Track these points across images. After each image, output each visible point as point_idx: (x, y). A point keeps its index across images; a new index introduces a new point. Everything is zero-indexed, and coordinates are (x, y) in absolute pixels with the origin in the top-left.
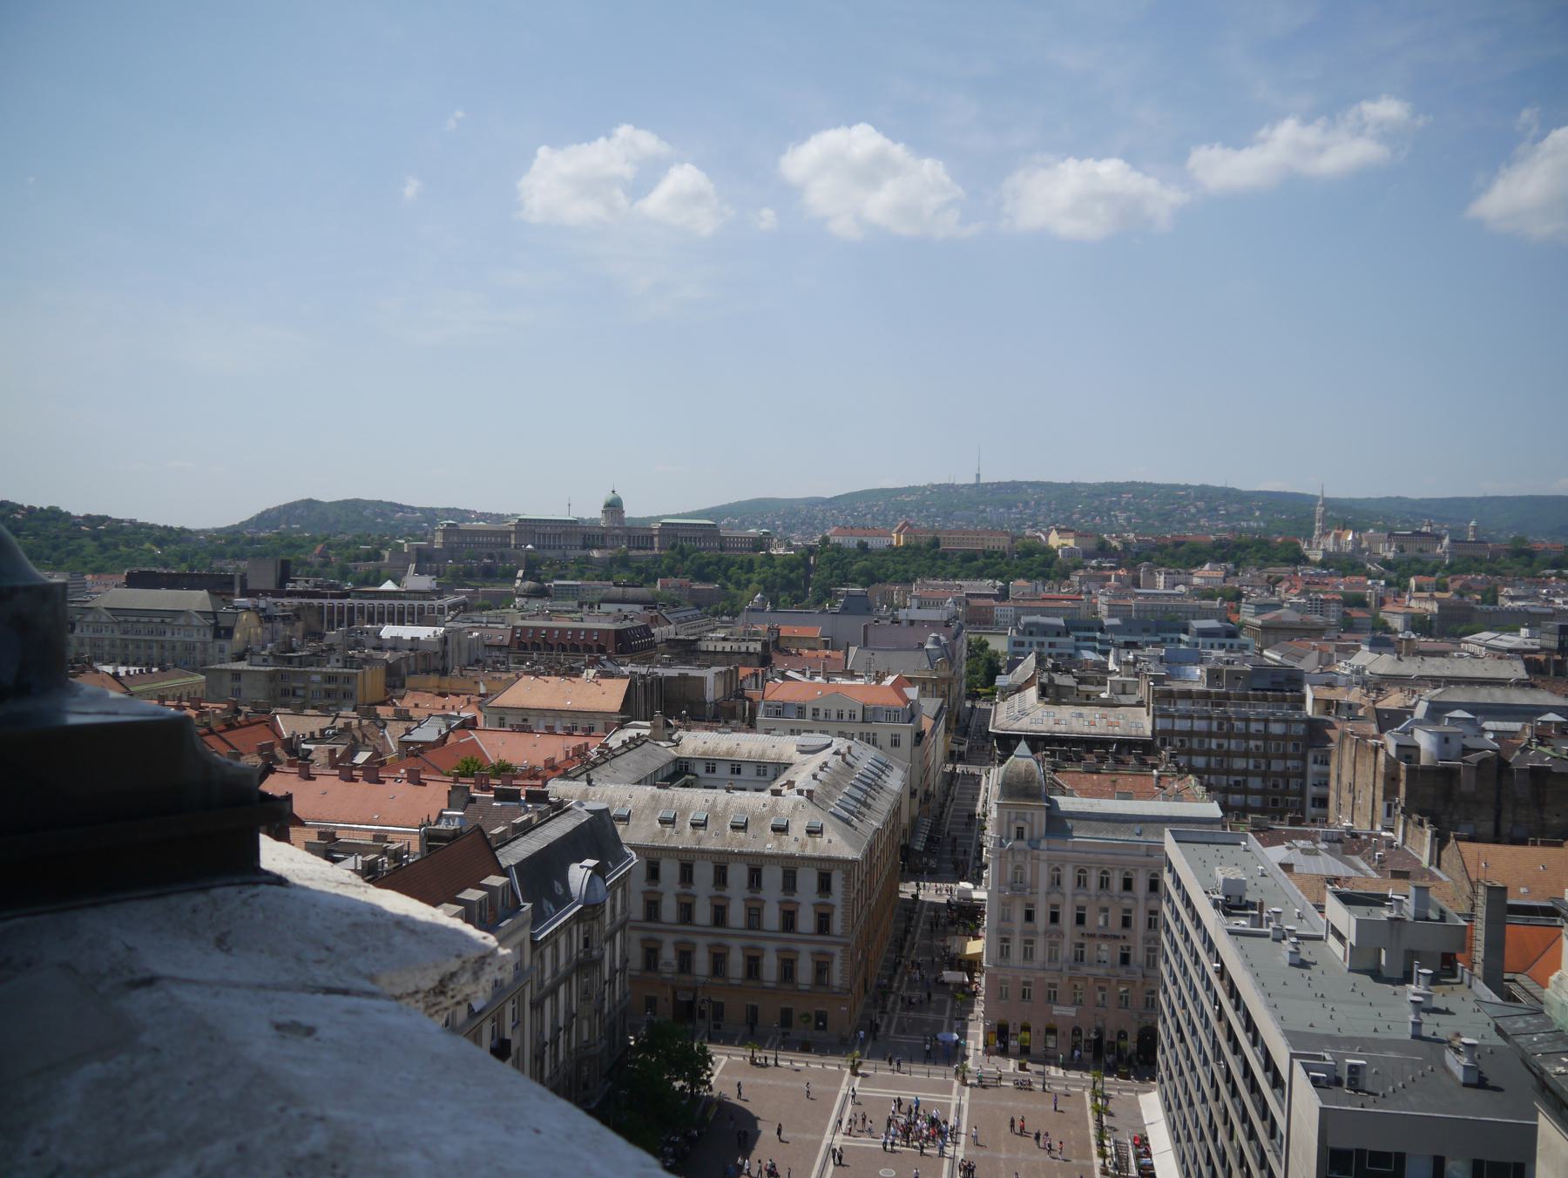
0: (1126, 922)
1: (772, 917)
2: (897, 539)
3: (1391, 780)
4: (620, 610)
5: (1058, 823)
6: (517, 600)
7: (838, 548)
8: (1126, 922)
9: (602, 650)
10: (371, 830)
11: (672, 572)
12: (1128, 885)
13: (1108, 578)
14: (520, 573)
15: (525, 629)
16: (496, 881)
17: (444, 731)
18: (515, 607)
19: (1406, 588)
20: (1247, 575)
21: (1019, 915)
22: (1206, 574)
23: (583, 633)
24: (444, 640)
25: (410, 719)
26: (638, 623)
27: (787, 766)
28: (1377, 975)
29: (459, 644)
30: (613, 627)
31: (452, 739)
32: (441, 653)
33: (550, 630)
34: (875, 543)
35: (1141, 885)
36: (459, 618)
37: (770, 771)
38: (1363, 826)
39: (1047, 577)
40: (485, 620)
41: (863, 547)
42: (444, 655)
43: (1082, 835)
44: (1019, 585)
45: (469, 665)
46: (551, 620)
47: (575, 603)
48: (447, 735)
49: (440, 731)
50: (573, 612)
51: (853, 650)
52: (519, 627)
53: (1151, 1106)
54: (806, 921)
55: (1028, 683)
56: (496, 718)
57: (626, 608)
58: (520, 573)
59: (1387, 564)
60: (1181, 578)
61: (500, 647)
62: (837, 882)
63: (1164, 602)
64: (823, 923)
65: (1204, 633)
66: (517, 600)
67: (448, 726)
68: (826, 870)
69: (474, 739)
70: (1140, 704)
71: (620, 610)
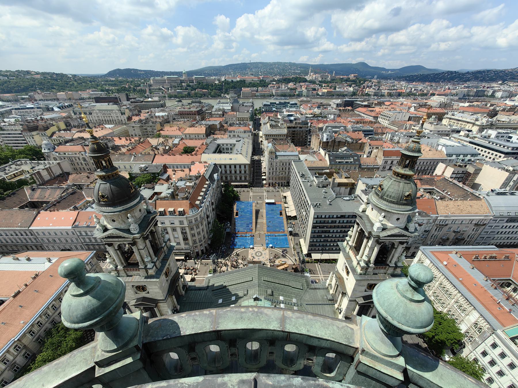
0: (286, 169)
1: (238, 172)
2: (238, 79)
3: (320, 143)
5: (276, 157)
7: (228, 81)
8: (286, 169)
9: (195, 114)
11: (198, 88)
12: (286, 165)
13: (274, 86)
16: (207, 183)
19: (322, 86)
20: (298, 85)
21: (271, 169)
22: (291, 85)
26: (200, 108)
27: (235, 145)
28: (319, 187)
33: (185, 111)
34: (234, 80)
35: (288, 164)
37: (232, 145)
38: (315, 150)
39: (264, 86)
41: (232, 81)
43: (279, 158)
44: (260, 88)
51: (238, 113)
53: (288, 194)
54: (243, 172)
55: (268, 122)
59: (320, 82)
60: (287, 86)
62: (247, 166)
63: (283, 91)
64: (245, 172)
65: (292, 104)
68: (245, 165)
70: (285, 128)
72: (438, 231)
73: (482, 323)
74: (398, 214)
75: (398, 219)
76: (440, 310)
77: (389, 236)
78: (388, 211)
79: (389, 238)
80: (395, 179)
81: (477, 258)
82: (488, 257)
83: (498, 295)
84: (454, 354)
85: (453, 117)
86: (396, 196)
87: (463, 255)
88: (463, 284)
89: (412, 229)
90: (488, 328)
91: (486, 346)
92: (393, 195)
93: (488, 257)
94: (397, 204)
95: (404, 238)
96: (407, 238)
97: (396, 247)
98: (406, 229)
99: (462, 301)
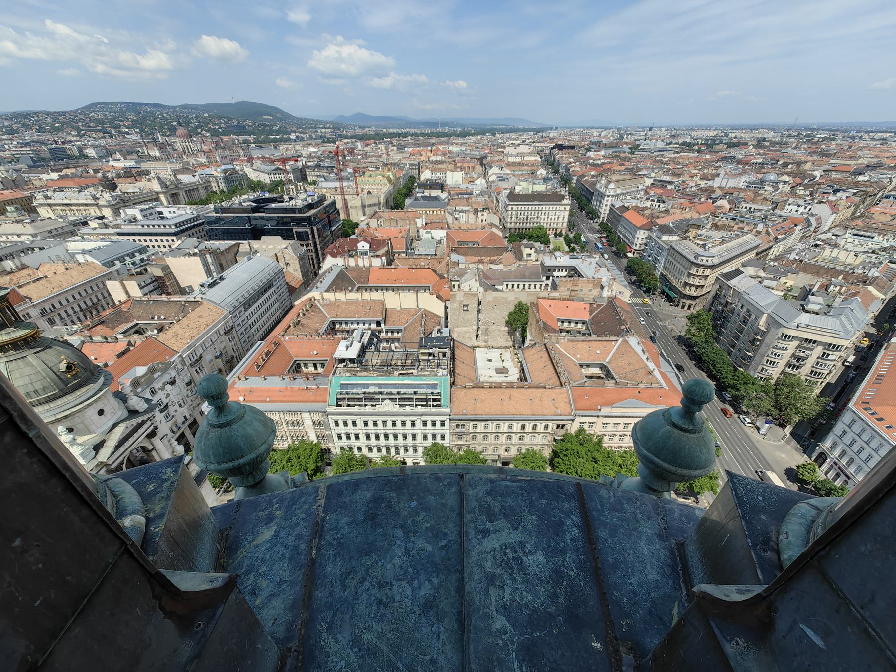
72: (201, 371)
73: (318, 417)
74: (89, 405)
75: (101, 412)
76: (287, 445)
77: (117, 448)
78: (66, 417)
79: (122, 449)
80: (6, 360)
81: (258, 366)
82: (265, 358)
83: (301, 382)
84: (329, 465)
85: (49, 201)
86: (46, 384)
87: (246, 375)
88: (273, 401)
89: (141, 405)
90: (322, 416)
91: (335, 431)
92: (38, 386)
93: (265, 358)
94: (66, 394)
95: (145, 427)
96: (149, 423)
97: (150, 447)
98: (133, 413)
99: (289, 417)
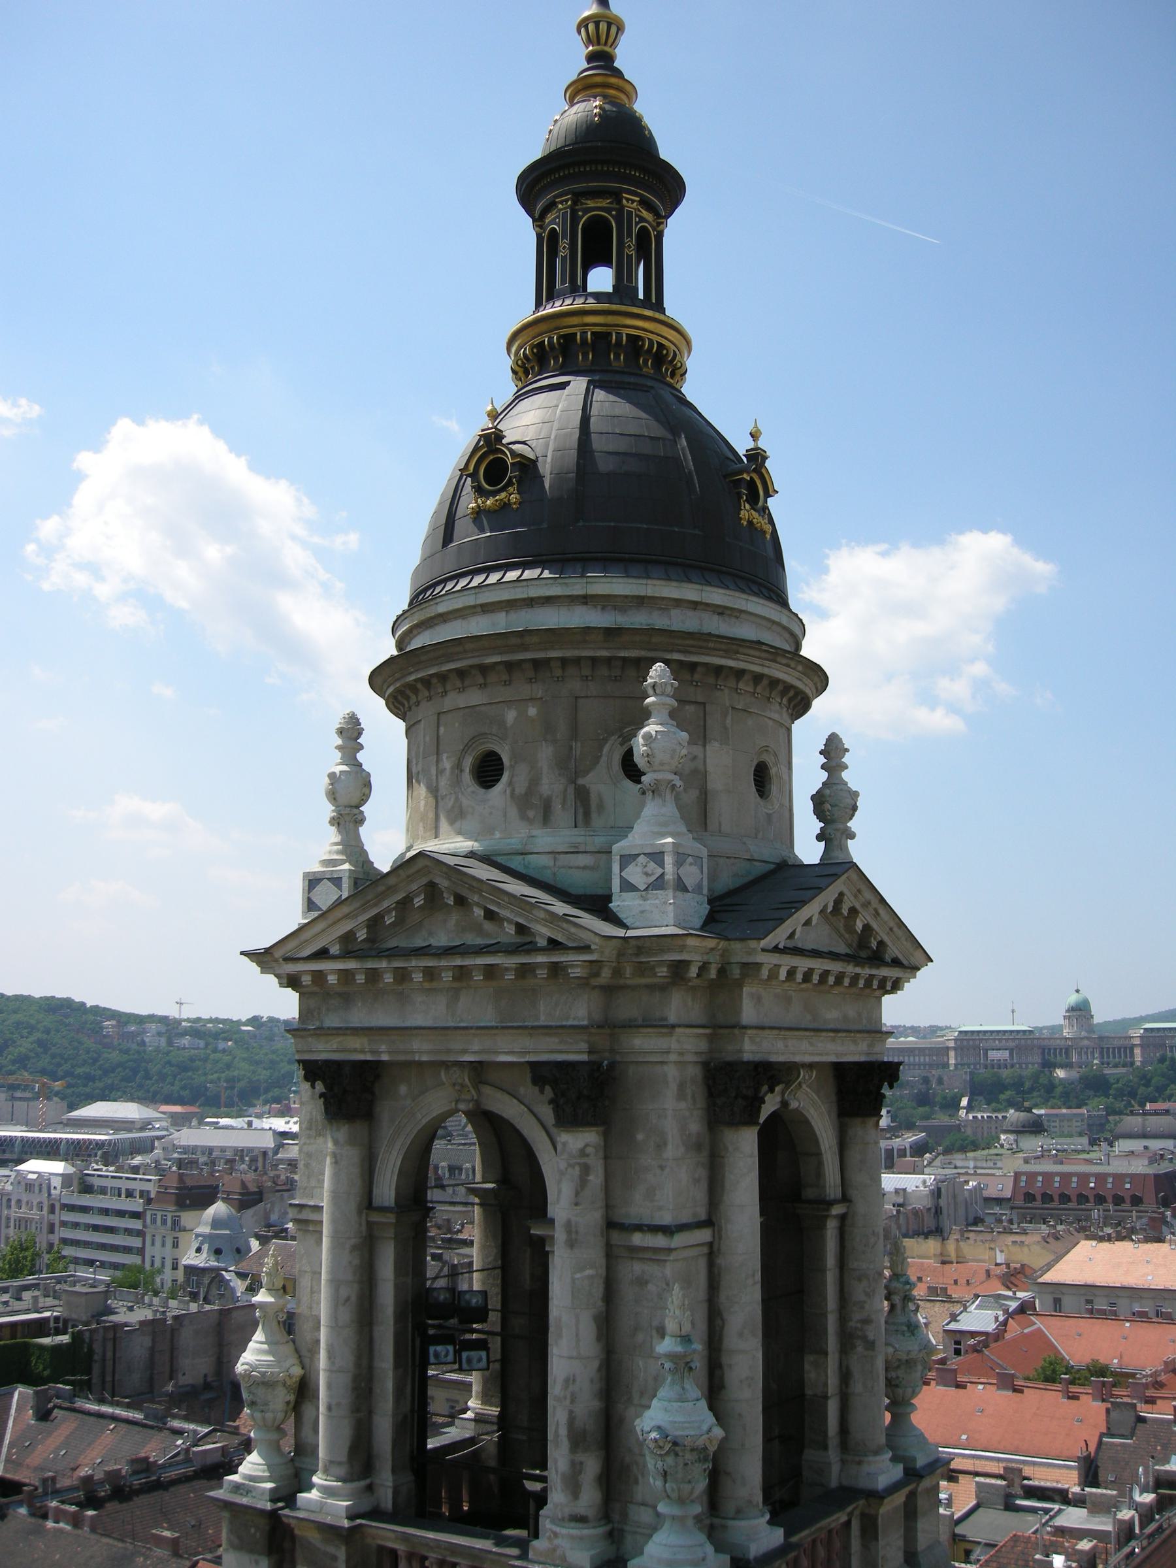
4: (1146, 1148)
6: (1003, 1137)
10: (999, 1460)
14: (964, 1102)
15: (1032, 1176)
17: (1001, 1318)
18: (1002, 1146)
23: (1110, 1180)
24: (937, 1193)
25: (950, 1300)
29: (955, 1197)
30: (1150, 1171)
31: (1014, 1328)
32: (933, 1210)
33: (1065, 1177)
36: (937, 1162)
40: (971, 1164)
42: (938, 1211)
45: (968, 1225)
46: (1062, 1163)
47: (1085, 1140)
48: (1005, 1323)
49: (997, 1318)
50: (1084, 1151)
52: (1025, 1173)
56: (1049, 1299)
57: (1156, 1145)
58: (964, 1102)
61: (999, 1201)
66: (1003, 1137)
67: (1006, 1311)
69: (1039, 1329)
71: (1146, 1148)
